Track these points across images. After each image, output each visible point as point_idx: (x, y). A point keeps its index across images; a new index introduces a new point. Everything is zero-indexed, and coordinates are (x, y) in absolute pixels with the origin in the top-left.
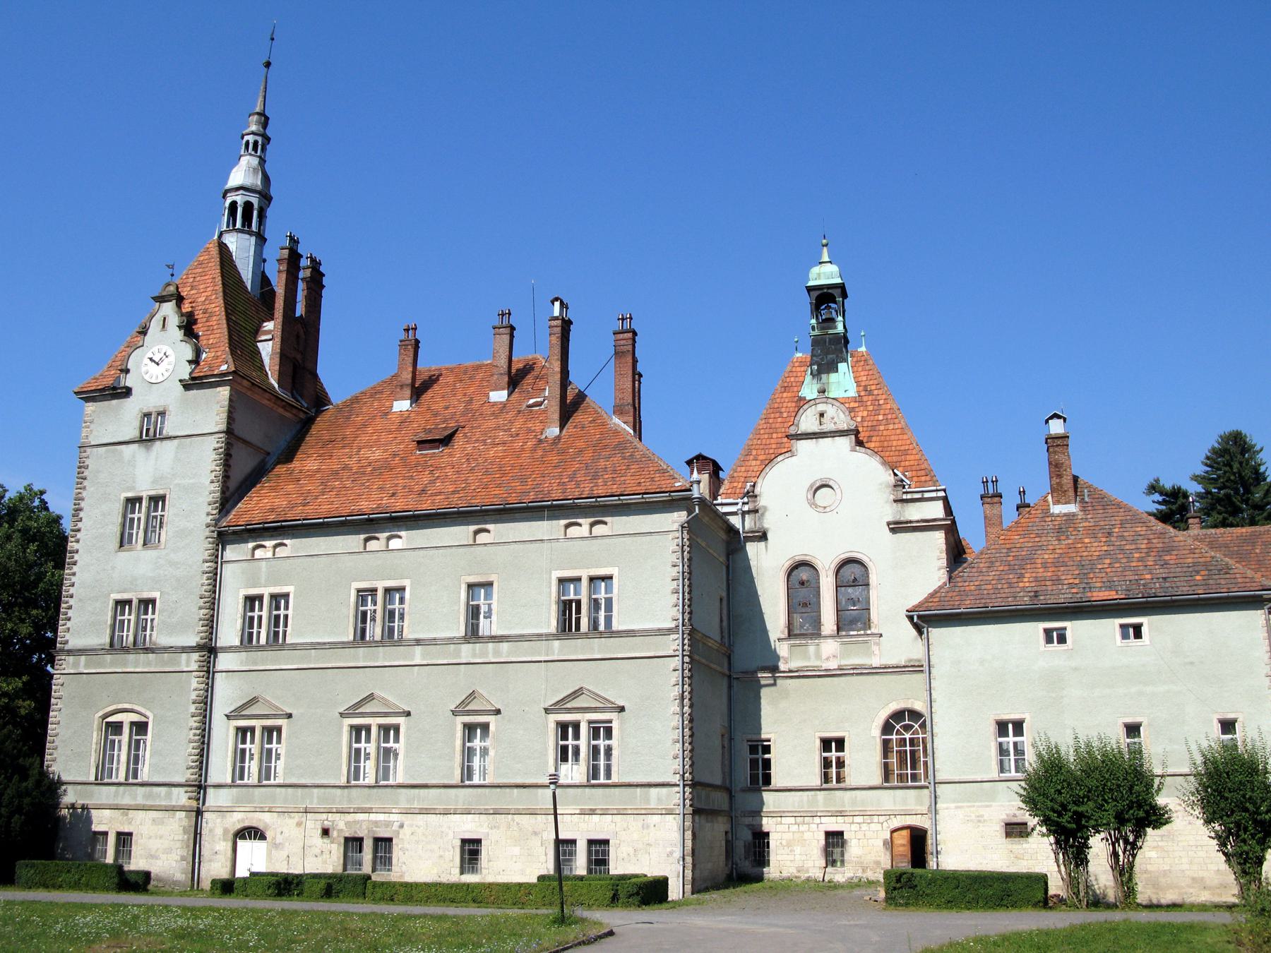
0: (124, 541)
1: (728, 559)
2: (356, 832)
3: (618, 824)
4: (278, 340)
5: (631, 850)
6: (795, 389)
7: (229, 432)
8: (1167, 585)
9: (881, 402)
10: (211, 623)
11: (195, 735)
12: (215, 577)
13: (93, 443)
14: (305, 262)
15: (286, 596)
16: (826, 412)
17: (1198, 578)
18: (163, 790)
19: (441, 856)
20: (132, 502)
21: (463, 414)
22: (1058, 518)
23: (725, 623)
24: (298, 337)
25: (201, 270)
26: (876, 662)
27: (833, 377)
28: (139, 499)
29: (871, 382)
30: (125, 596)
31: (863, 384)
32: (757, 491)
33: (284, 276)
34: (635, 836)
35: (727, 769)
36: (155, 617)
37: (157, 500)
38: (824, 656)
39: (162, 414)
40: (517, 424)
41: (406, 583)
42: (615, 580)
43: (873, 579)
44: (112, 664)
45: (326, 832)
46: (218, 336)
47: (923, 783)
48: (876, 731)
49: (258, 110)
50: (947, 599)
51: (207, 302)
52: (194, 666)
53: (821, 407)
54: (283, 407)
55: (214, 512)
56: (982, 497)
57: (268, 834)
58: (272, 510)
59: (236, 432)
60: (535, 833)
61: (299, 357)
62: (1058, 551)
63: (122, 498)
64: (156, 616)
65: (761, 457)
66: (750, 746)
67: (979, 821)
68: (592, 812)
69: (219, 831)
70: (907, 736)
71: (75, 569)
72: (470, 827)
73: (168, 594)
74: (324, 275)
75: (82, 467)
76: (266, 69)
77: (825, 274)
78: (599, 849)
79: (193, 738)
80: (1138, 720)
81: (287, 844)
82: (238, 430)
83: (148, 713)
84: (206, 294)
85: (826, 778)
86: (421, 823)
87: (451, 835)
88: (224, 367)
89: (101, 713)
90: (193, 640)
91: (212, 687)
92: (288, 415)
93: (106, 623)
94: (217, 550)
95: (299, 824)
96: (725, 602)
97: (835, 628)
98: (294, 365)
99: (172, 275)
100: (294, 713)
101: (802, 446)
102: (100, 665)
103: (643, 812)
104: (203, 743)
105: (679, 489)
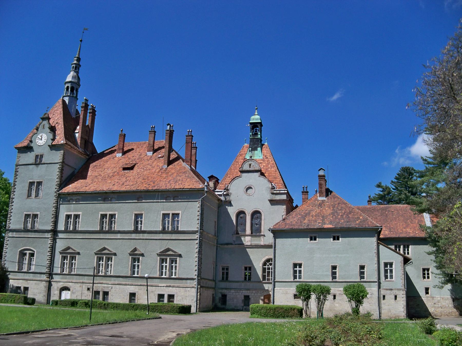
0: (29, 195)
1: (218, 209)
4: (80, 133)
5: (181, 298)
6: (244, 155)
7: (63, 162)
8: (348, 224)
9: (270, 161)
10: (56, 223)
11: (49, 258)
13: (20, 164)
14: (90, 107)
15: (79, 215)
16: (252, 164)
17: (357, 222)
18: (39, 275)
19: (123, 298)
20: (31, 184)
21: (138, 159)
22: (320, 201)
23: (216, 229)
24: (87, 131)
25: (56, 109)
26: (262, 243)
27: (256, 152)
28: (34, 182)
29: (268, 154)
30: (29, 213)
31: (265, 155)
32: (229, 188)
33: (83, 112)
34: (182, 294)
35: (215, 275)
36: (38, 220)
37: (39, 183)
38: (246, 241)
39: (42, 156)
40: (154, 164)
41: (116, 213)
42: (180, 215)
43: (263, 217)
44: (24, 235)
45: (88, 289)
46: (61, 131)
47: (271, 281)
48: (261, 265)
49: (77, 56)
50: (281, 225)
51: (58, 120)
52: (50, 236)
53: (250, 162)
54: (81, 154)
55: (58, 188)
56: (302, 192)
57: (71, 289)
58: (75, 188)
59: (66, 162)
60: (152, 292)
61: (87, 138)
62: (317, 212)
63: (29, 182)
64: (38, 220)
65: (231, 177)
66: (222, 268)
67: (286, 293)
68: (170, 286)
69: (56, 288)
70: (271, 267)
71: (13, 204)
72: (132, 289)
73: (42, 213)
74: (96, 111)
75: (16, 171)
77: (256, 118)
78: (171, 297)
79: (48, 258)
80: (336, 265)
83: (35, 250)
84: (58, 117)
85: (245, 278)
86: (118, 287)
87: (127, 291)
88: (62, 142)
89: (20, 250)
90: (50, 228)
92: (82, 157)
93: (22, 221)
94: (58, 200)
95: (80, 286)
96: (216, 223)
97: (250, 232)
98: (85, 141)
100: (81, 252)
101: (244, 175)
105: (201, 187)
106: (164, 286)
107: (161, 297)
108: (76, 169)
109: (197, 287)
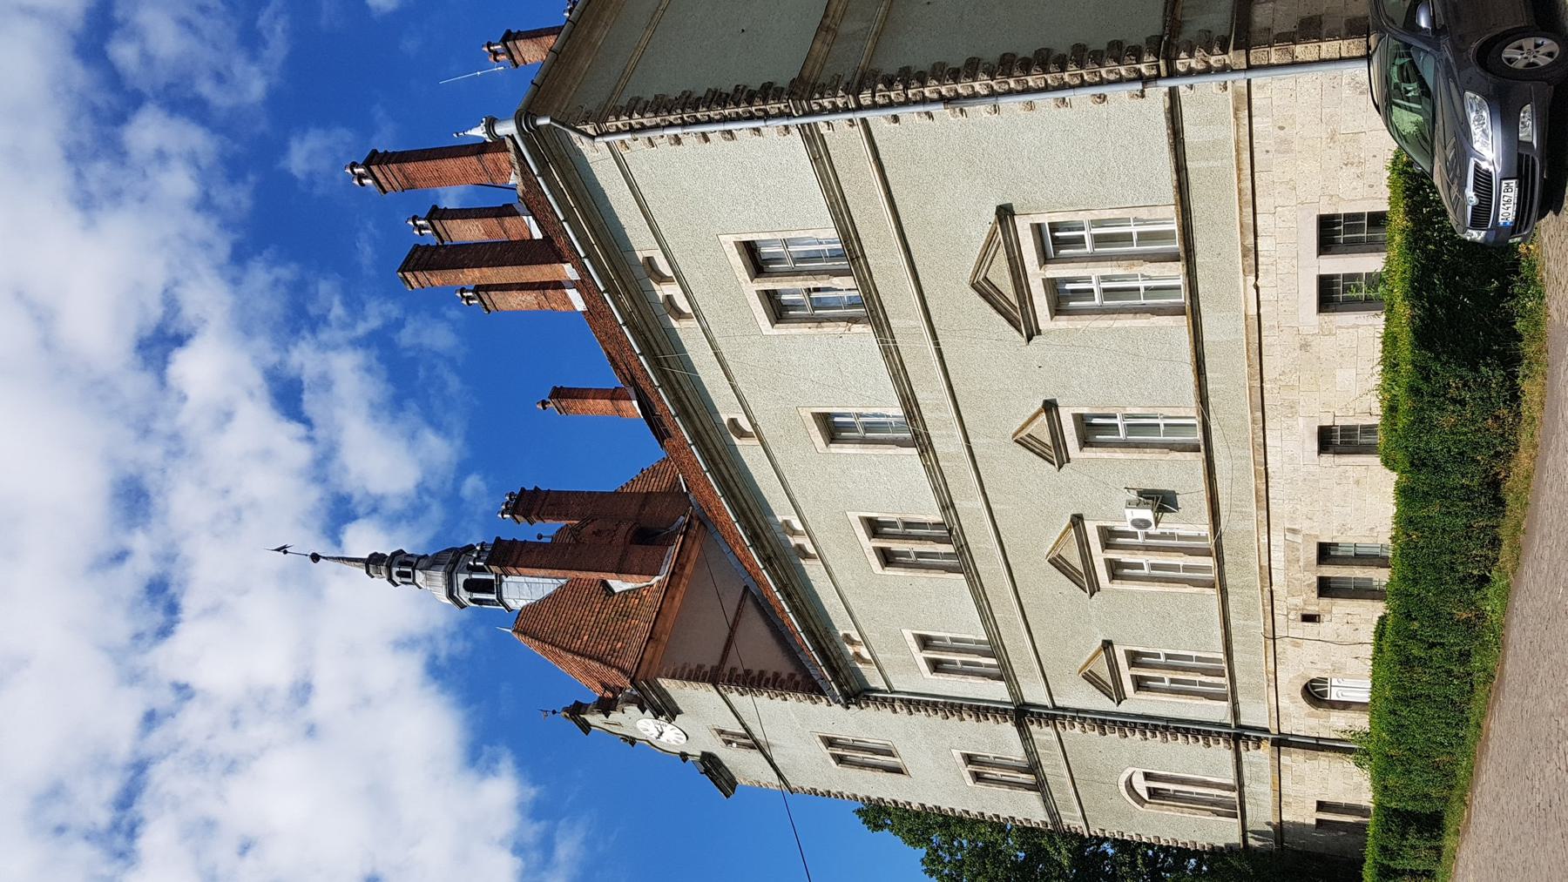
2: (1309, 585)
3: (1279, 201)
12: (914, 703)
24: (597, 533)
41: (854, 517)
44: (1062, 790)
45: (1308, 618)
59: (716, 663)
60: (1305, 346)
61: (624, 528)
69: (1313, 722)
76: (321, 560)
81: (1333, 658)
82: (710, 660)
91: (1078, 711)
99: (554, 712)
102: (1068, 800)
103: (1246, 156)
104: (1166, 728)
106: (1257, 288)
107: (1330, 295)
108: (746, 589)
109: (1242, 75)
